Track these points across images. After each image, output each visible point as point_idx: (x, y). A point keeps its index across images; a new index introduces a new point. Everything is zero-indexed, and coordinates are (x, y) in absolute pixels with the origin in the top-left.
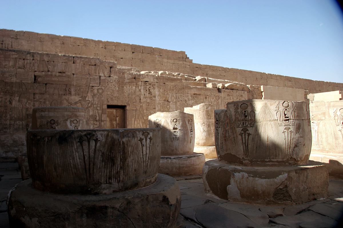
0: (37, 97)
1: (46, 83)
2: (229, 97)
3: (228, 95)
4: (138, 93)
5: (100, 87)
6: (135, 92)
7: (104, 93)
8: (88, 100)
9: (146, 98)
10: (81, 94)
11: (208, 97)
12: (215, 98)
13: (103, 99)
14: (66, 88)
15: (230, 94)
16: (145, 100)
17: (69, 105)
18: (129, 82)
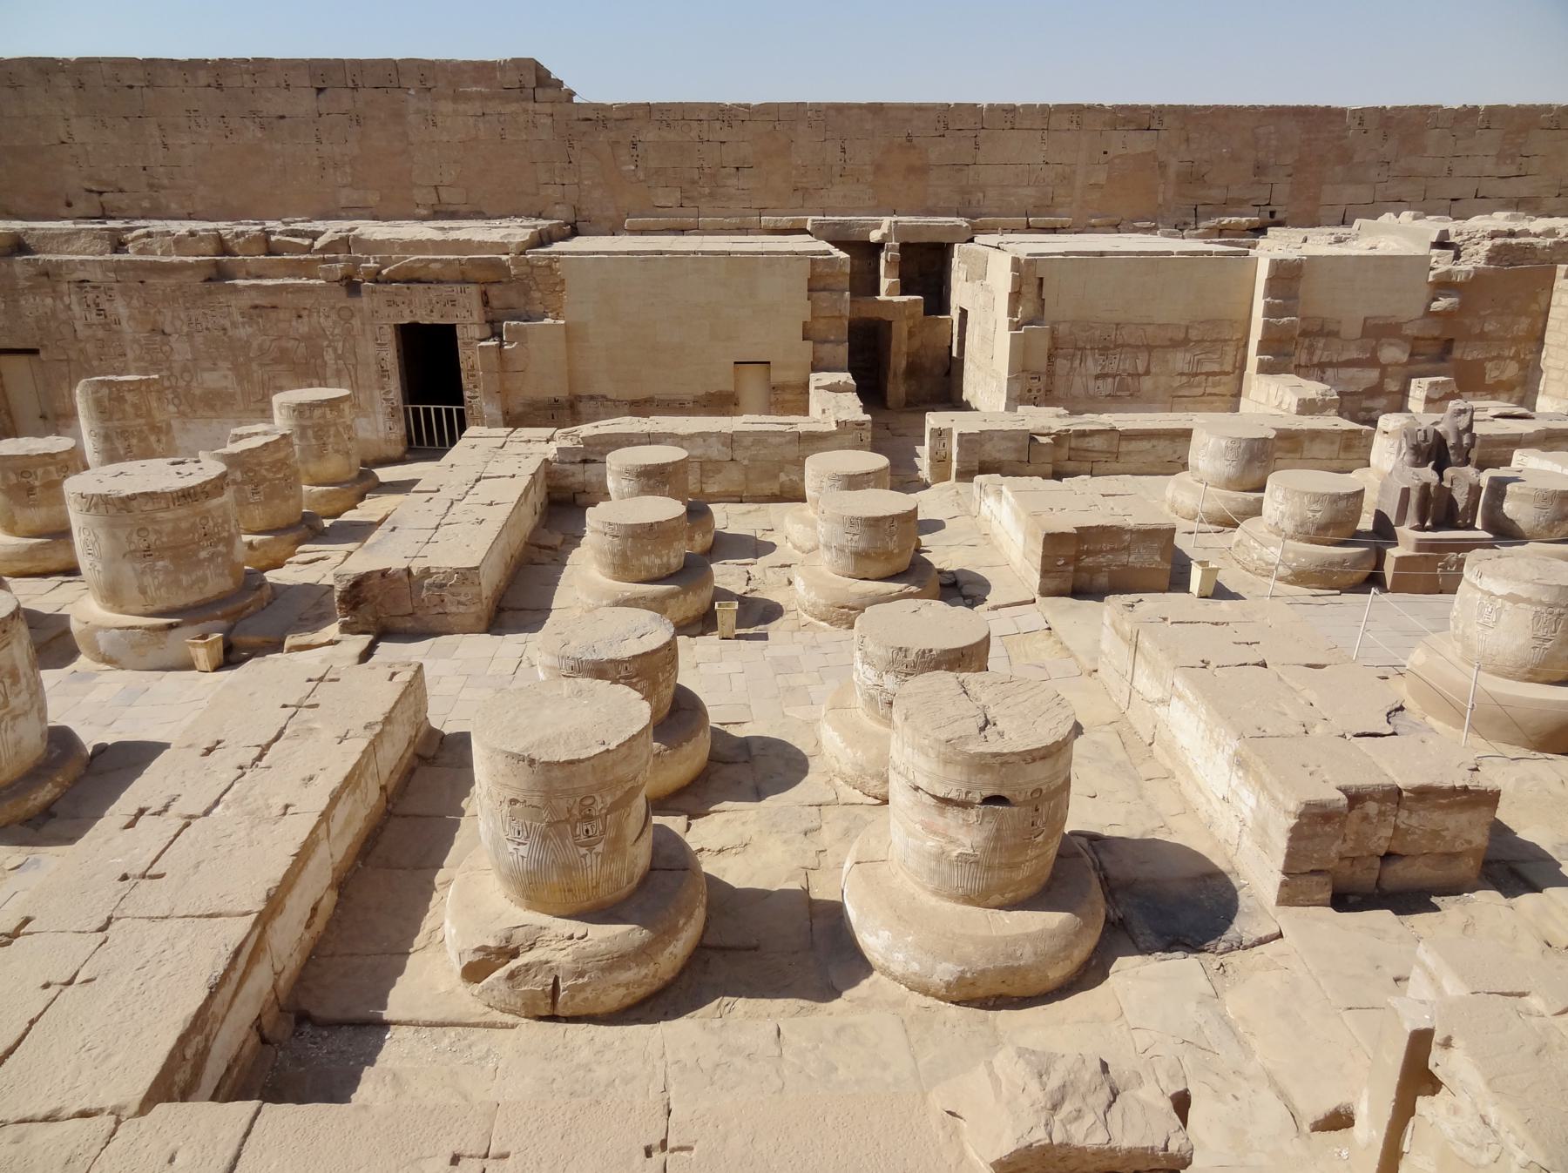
2: (393, 311)
3: (391, 303)
4: (63, 316)
6: (54, 312)
9: (89, 326)
11: (305, 313)
12: (334, 317)
15: (398, 299)
16: (89, 332)
18: (31, 287)
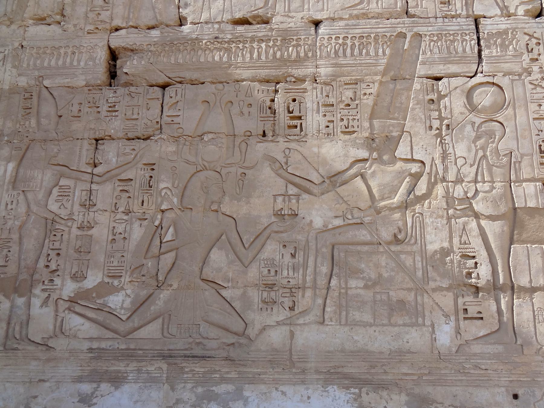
0: (111, 154)
1: (162, 79)
5: (479, 78)
7: (510, 111)
8: (413, 160)
10: (366, 124)
13: (513, 145)
14: (273, 101)
17: (292, 190)
